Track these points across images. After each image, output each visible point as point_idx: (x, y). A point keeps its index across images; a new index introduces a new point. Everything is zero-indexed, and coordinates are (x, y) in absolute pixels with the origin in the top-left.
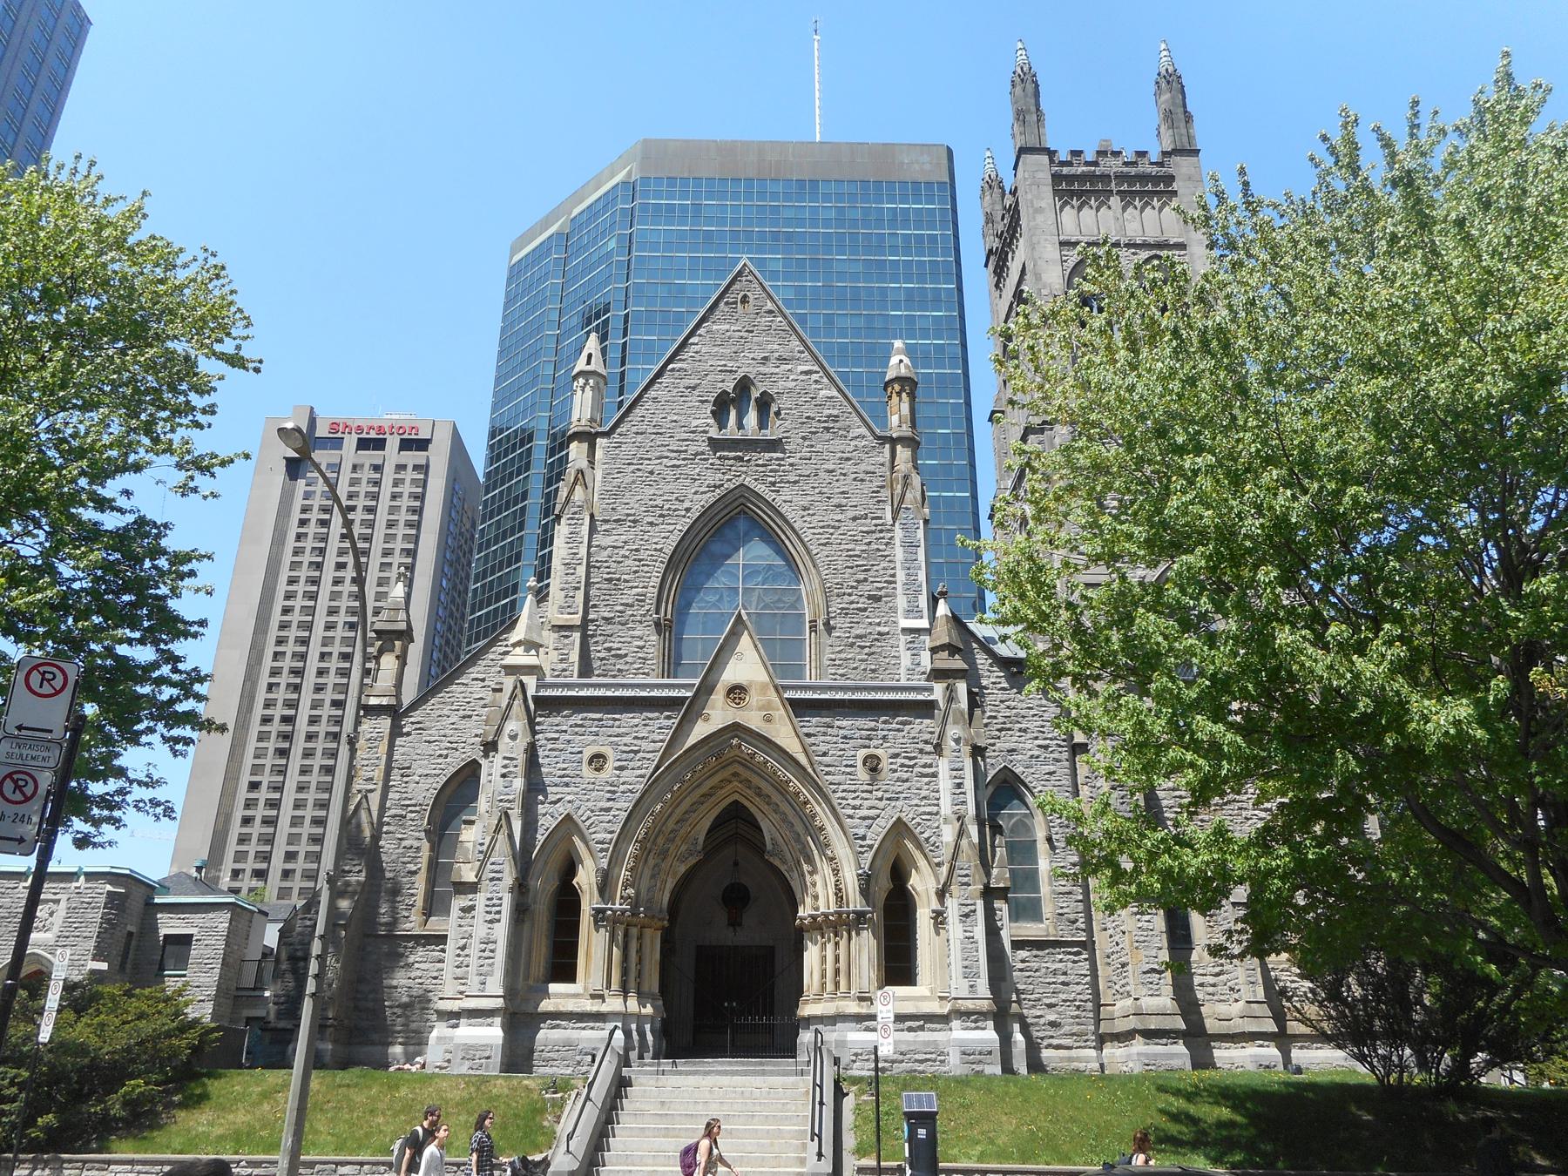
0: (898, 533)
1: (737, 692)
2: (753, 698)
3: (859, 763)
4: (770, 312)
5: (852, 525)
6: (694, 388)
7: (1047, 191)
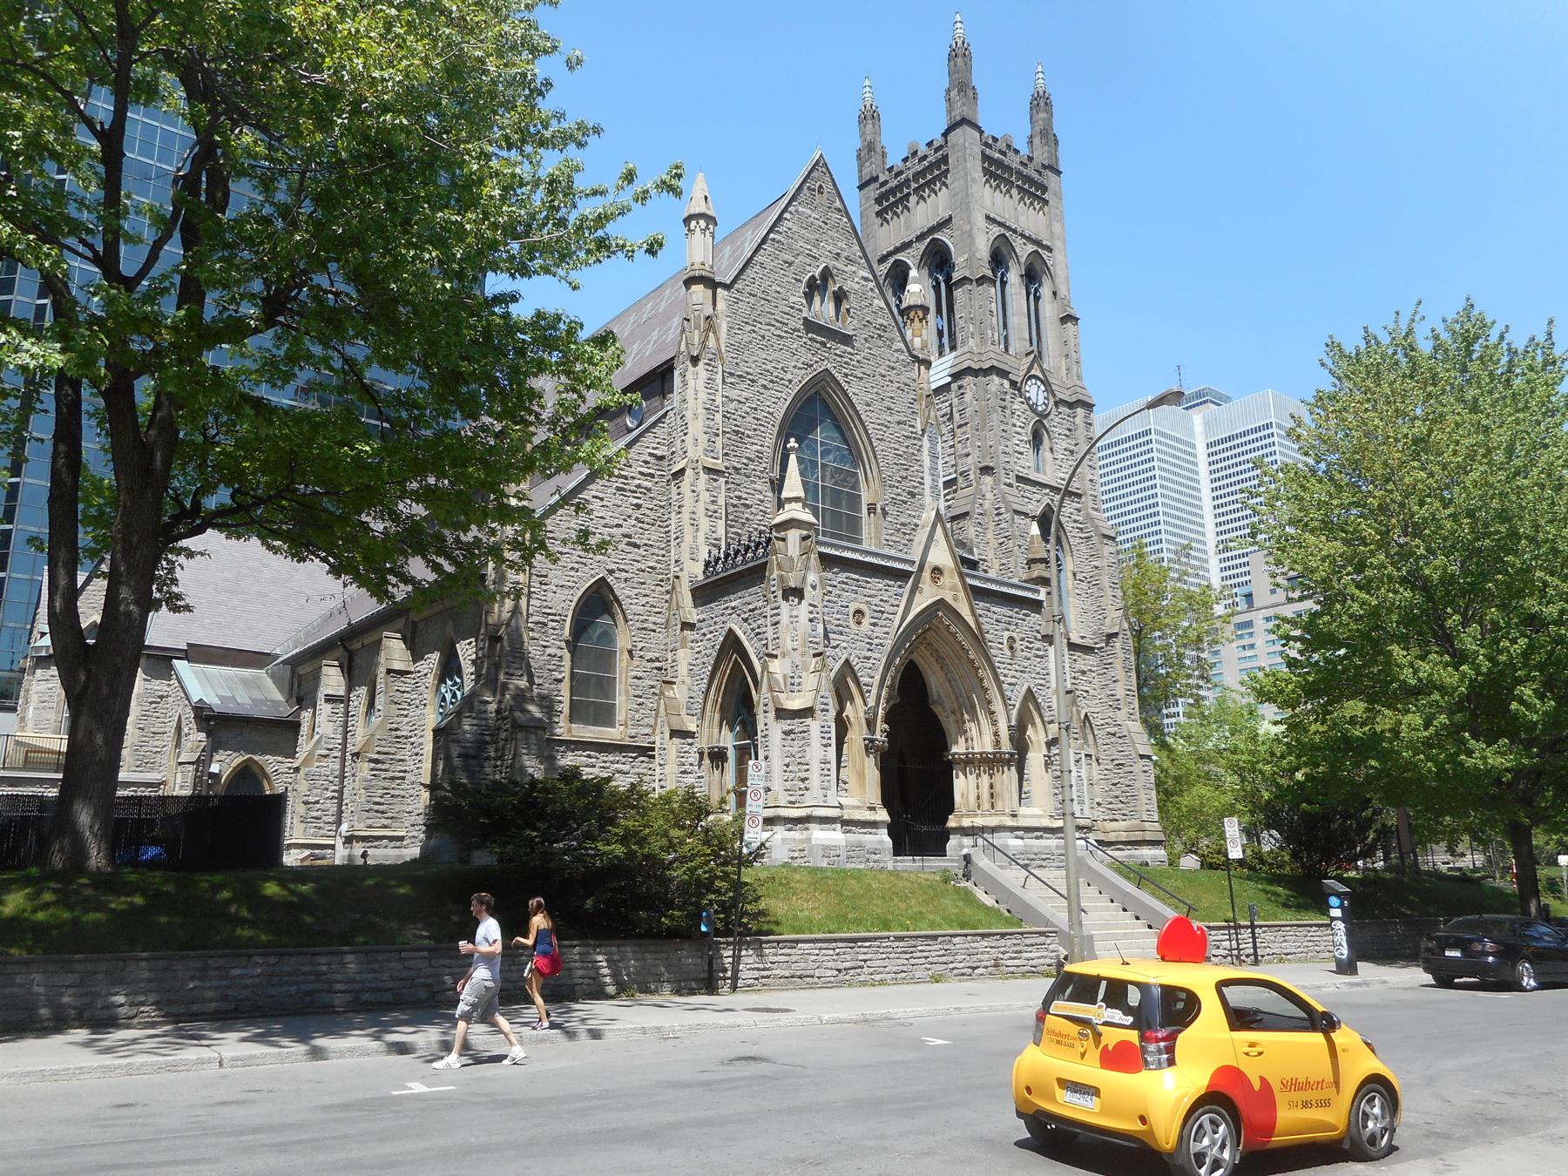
0: (926, 442)
6: (790, 264)
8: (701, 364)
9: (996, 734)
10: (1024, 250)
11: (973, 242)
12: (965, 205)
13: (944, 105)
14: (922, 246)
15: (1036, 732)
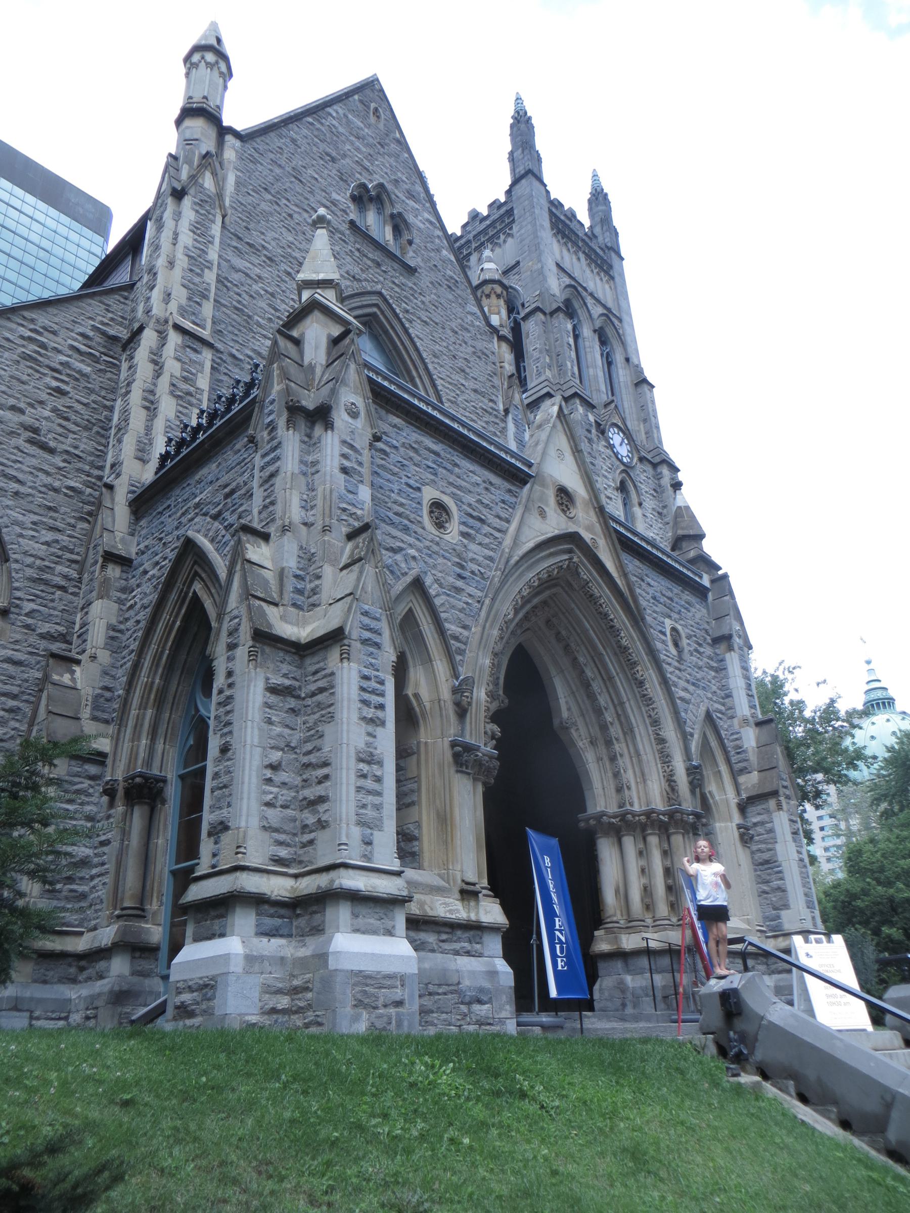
3: (668, 633)
6: (333, 160)
9: (670, 780)
12: (536, 248)
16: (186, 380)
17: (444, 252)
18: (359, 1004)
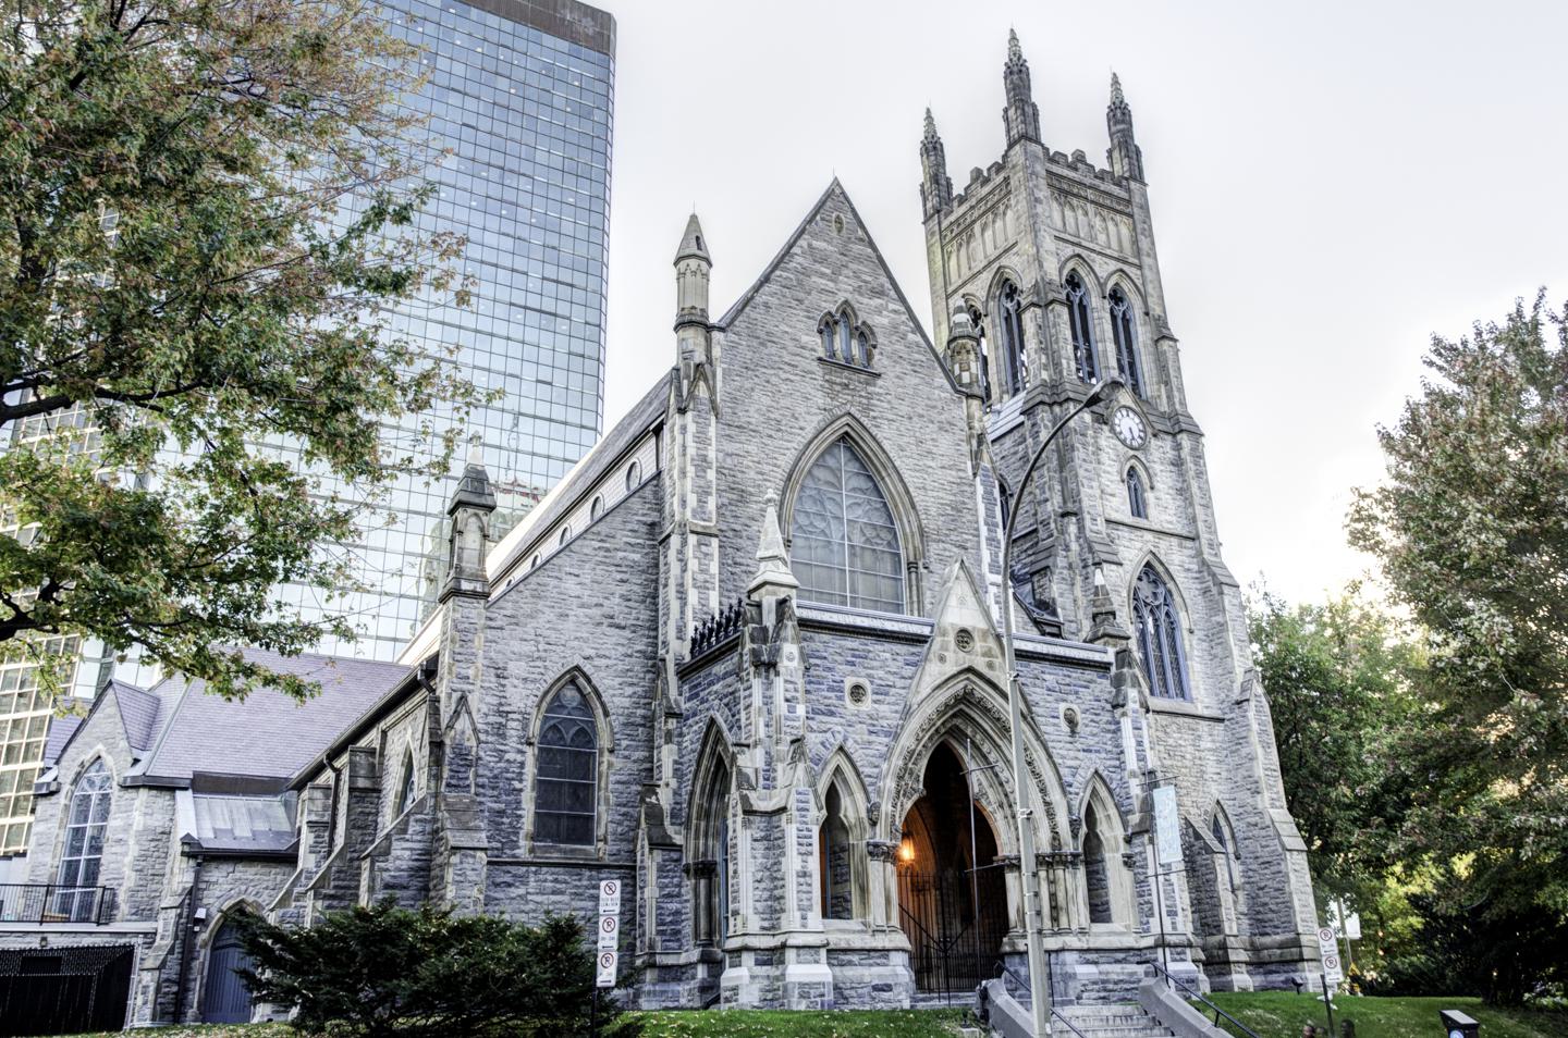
1: (964, 637)
2: (978, 645)
4: (862, 240)
5: (939, 472)
7: (1043, 183)
8: (689, 415)
10: (1104, 268)
11: (1041, 266)
13: (1002, 126)
14: (987, 276)
15: (1111, 828)
16: (702, 571)
17: (911, 337)
18: (801, 996)
